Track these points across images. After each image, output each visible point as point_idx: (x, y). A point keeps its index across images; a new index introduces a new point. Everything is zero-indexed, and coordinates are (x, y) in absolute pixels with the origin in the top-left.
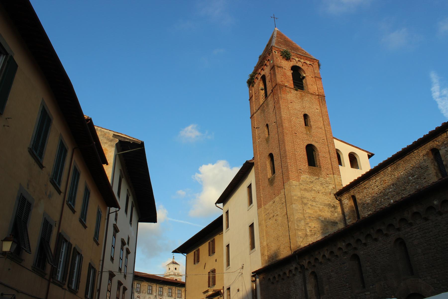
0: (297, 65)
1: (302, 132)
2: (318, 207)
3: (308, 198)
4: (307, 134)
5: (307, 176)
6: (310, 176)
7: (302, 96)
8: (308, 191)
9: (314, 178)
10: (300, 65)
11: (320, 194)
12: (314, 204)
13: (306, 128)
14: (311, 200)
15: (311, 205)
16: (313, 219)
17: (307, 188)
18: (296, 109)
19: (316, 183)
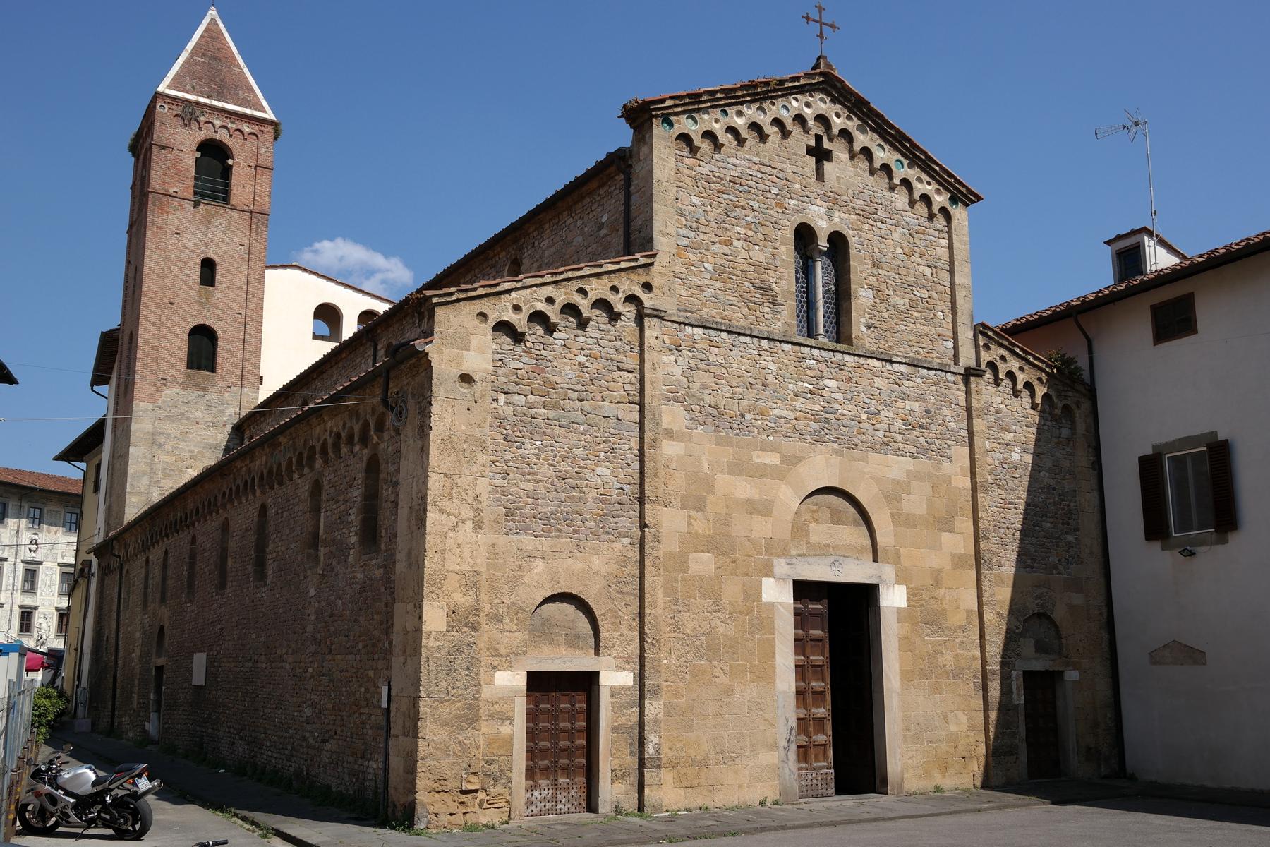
1: (187, 300)
2: (190, 451)
4: (199, 303)
5: (181, 392)
9: (193, 395)
10: (222, 136)
11: (201, 426)
12: (182, 445)
16: (172, 472)
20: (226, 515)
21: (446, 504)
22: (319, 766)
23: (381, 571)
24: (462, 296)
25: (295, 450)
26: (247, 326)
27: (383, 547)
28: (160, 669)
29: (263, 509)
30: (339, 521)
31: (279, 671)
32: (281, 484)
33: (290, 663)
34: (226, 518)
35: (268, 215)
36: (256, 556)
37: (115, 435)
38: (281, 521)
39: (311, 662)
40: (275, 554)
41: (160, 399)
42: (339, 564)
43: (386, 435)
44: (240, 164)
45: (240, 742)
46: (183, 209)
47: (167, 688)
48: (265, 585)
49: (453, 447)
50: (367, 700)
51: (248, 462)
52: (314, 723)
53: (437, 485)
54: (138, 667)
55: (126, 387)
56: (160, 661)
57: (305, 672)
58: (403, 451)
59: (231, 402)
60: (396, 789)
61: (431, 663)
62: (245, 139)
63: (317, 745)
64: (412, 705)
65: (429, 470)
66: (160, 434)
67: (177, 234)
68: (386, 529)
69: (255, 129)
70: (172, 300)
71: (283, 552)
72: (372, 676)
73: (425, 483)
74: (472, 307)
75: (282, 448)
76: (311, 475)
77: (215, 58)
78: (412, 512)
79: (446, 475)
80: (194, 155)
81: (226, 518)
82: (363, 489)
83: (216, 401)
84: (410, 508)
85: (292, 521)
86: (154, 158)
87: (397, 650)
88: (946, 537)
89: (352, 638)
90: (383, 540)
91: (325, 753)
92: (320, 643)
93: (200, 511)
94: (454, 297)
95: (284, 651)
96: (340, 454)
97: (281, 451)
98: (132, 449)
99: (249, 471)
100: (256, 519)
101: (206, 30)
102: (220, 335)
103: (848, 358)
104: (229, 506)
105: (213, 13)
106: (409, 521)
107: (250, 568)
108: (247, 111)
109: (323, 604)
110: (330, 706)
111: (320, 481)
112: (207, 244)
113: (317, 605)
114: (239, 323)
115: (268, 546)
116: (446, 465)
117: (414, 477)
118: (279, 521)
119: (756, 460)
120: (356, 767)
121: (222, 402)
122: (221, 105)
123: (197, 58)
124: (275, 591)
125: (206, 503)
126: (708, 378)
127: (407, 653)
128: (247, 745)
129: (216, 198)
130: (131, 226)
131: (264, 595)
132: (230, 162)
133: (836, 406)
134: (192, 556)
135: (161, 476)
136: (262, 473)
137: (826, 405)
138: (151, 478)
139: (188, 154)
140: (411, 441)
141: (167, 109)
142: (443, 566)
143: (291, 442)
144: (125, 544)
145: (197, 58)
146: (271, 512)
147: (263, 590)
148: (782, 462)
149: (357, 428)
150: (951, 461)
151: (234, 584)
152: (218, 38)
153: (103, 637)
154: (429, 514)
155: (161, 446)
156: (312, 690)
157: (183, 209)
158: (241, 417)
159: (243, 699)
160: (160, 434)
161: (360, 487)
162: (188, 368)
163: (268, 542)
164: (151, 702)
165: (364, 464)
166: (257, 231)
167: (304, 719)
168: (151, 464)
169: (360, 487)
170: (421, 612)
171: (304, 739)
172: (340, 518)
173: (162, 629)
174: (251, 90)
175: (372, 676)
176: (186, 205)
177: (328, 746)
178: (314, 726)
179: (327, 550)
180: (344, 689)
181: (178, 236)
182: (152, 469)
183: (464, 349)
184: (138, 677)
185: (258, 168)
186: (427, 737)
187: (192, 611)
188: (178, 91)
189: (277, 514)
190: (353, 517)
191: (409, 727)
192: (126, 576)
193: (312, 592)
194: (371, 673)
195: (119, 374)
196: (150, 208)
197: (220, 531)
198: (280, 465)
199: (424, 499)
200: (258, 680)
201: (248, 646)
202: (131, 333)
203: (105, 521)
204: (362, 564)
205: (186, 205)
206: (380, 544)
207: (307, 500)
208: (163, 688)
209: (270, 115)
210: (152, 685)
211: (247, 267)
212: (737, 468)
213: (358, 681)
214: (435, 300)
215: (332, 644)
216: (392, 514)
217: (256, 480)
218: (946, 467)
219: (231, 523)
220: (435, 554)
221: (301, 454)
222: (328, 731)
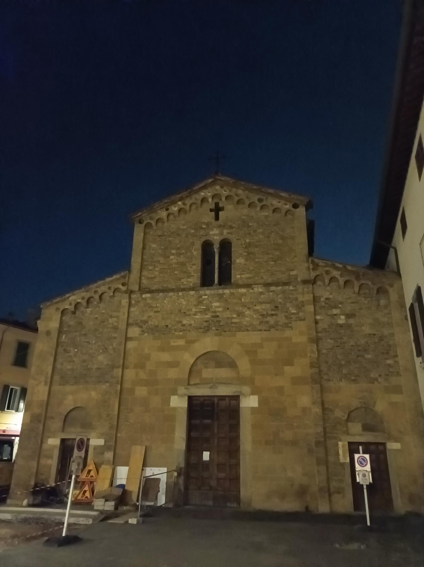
88: (287, 369)
103: (227, 291)
119: (172, 344)
126: (152, 314)
133: (218, 314)
137: (213, 314)
148: (186, 343)
150: (292, 329)
212: (162, 349)
218: (288, 333)
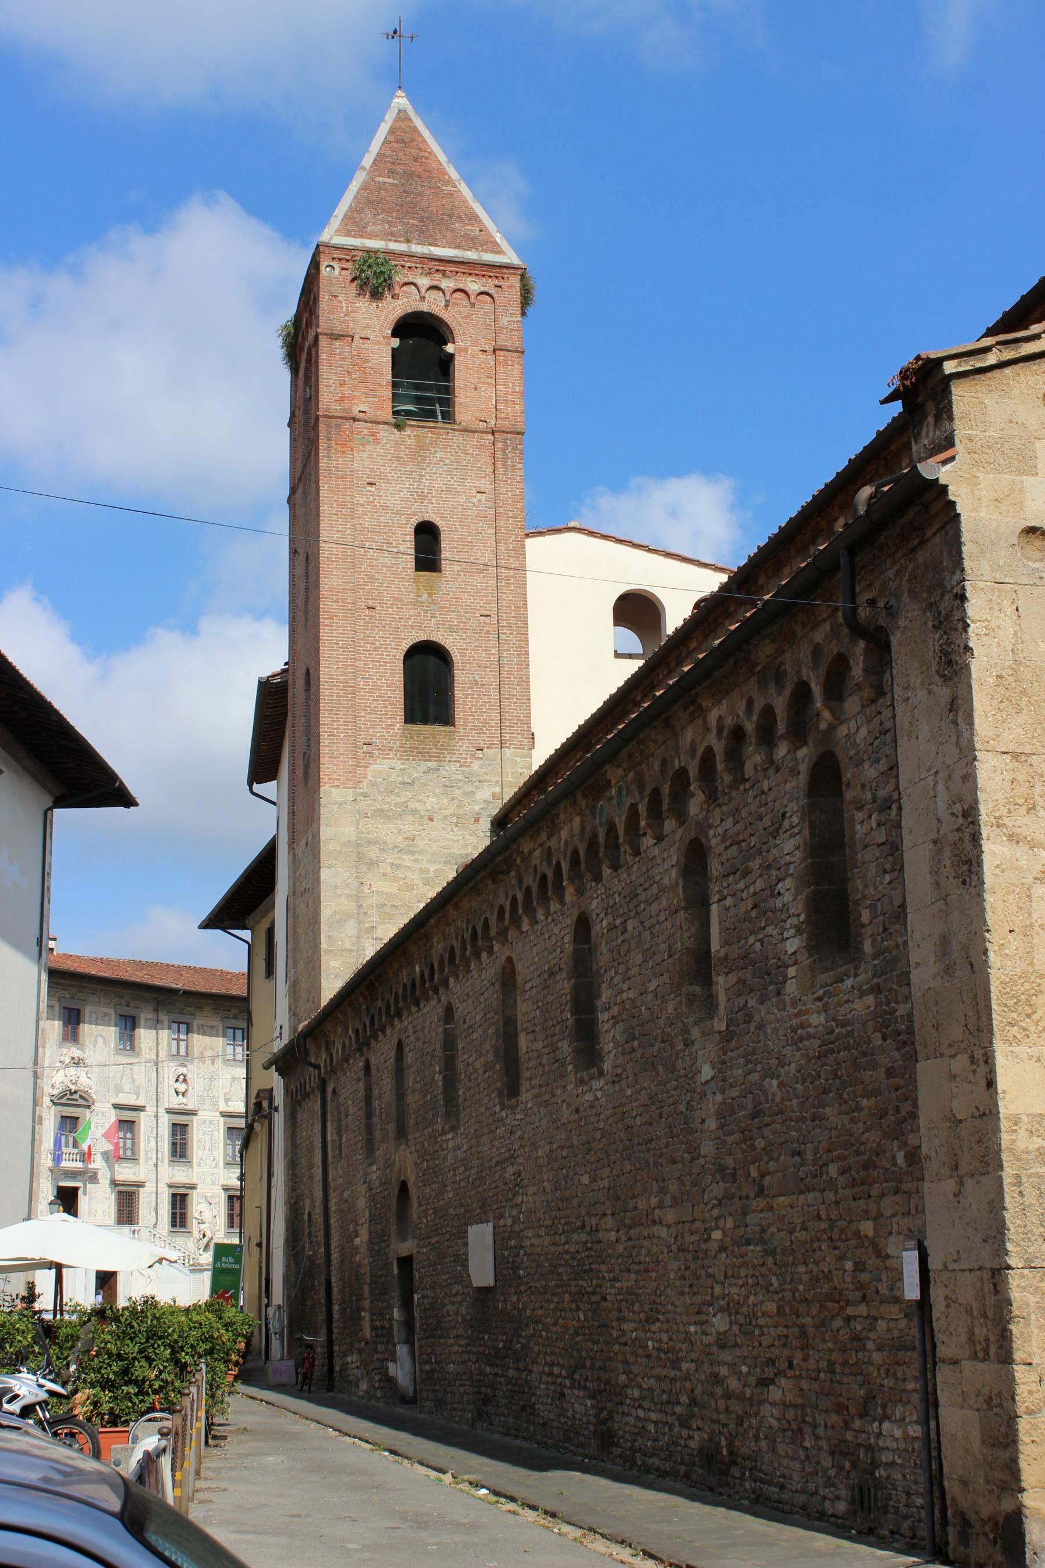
0: (425, 307)
1: (396, 599)
2: (422, 871)
3: (385, 842)
4: (416, 603)
5: (398, 765)
6: (403, 764)
7: (421, 448)
8: (388, 818)
9: (419, 769)
10: (434, 304)
12: (407, 860)
13: (416, 581)
14: (396, 847)
15: (392, 864)
16: (395, 911)
17: (387, 807)
18: (385, 508)
19: (426, 785)
20: (508, 953)
21: (1021, 822)
22: (757, 1437)
23: (870, 1000)
24: (1008, 354)
25: (641, 787)
26: (502, 636)
27: (867, 947)
28: (406, 1262)
29: (583, 926)
30: (754, 913)
31: (646, 1243)
32: (616, 867)
33: (669, 1226)
34: (509, 960)
35: (523, 434)
36: (576, 1021)
37: (294, 856)
38: (623, 941)
39: (717, 1218)
40: (615, 1010)
41: (365, 781)
42: (762, 1003)
43: (852, 704)
44: (466, 350)
45: (576, 1392)
46: (376, 441)
47: (424, 1297)
48: (601, 1073)
49: (1023, 692)
50: (861, 1287)
51: (544, 836)
52: (736, 1345)
53: (998, 778)
54: (366, 1261)
55: (306, 767)
56: (406, 1248)
57: (706, 1241)
58: (903, 720)
59: (485, 777)
60: (964, 1483)
61: (1027, 1189)
62: (473, 305)
63: (748, 1392)
64: (988, 1287)
65: (977, 746)
66: (370, 843)
67: (371, 484)
68: (873, 907)
69: (489, 285)
70: (371, 603)
71: (633, 1001)
72: (871, 1233)
73: (970, 778)
74: (1032, 379)
75: (614, 791)
76: (680, 832)
77: (410, 175)
78: (939, 852)
79: (1015, 756)
80: (387, 344)
81: (509, 960)
82: (806, 832)
83: (460, 777)
84: (935, 842)
85: (647, 935)
86: (323, 357)
87: (932, 1167)
89: (809, 1156)
90: (868, 931)
91: (768, 1407)
92: (734, 1175)
93: (458, 952)
94: (991, 359)
95: (654, 1201)
96: (743, 774)
97: (611, 798)
98: (324, 874)
99: (549, 853)
100: (569, 948)
101: (392, 131)
102: (456, 657)
104: (512, 933)
105: (401, 101)
106: (935, 873)
107: (566, 1047)
108: (471, 255)
109: (734, 1092)
110: (771, 1307)
111: (703, 840)
112: (422, 497)
113: (719, 1098)
114: (488, 632)
115: (599, 997)
116: (1012, 736)
117: (937, 773)
118: (619, 941)
120: (849, 1436)
121: (469, 779)
122: (426, 252)
123: (380, 179)
124: (624, 1082)
125: (467, 936)
127: (964, 1169)
128: (592, 1397)
129: (431, 415)
130: (293, 490)
131: (599, 1094)
132: (450, 348)
134: (449, 1044)
135: (376, 918)
136: (575, 853)
138: (359, 923)
139: (379, 343)
140: (922, 695)
141: (337, 270)
142: (1032, 964)
143: (631, 775)
144: (327, 1043)
145: (380, 179)
146: (600, 926)
147: (597, 1084)
149: (780, 704)
151: (536, 1082)
152: (412, 140)
153: (303, 1214)
154: (986, 846)
155: (372, 864)
156: (726, 1276)
157: (376, 441)
158: (505, 801)
159: (573, 1306)
160: (370, 843)
161: (796, 830)
162: (406, 722)
163: (599, 987)
164: (395, 1324)
165: (803, 779)
166: (505, 464)
167: (710, 1339)
168: (358, 898)
169: (796, 830)
170: (992, 1071)
171: (717, 1379)
172: (755, 906)
173: (404, 1187)
174: (475, 219)
175: (871, 1233)
176: (382, 433)
177: (775, 1393)
178: (738, 1352)
179: (733, 978)
180: (801, 1269)
181: (373, 489)
182: (360, 907)
183: (1022, 473)
184: (368, 1281)
185: (498, 353)
186: (1034, 1362)
187: (458, 1147)
188: (354, 237)
189: (612, 928)
190: (787, 897)
191: (987, 1340)
192: (332, 1101)
193: (707, 1072)
194: (867, 1228)
195: (293, 751)
196: (323, 445)
197: (498, 985)
198: (611, 829)
199: (970, 814)
200: (603, 1267)
201: (576, 1201)
202: (308, 673)
203: (290, 1009)
204: (821, 992)
205: (382, 433)
206: (861, 943)
207: (677, 884)
208: (416, 1297)
209: (510, 257)
210: (396, 1294)
211: (493, 531)
213: (835, 1248)
214: (949, 367)
215: (763, 1176)
216: (885, 872)
217: (565, 867)
219: (519, 967)
220: (1010, 936)
221: (656, 793)
222: (771, 1362)
